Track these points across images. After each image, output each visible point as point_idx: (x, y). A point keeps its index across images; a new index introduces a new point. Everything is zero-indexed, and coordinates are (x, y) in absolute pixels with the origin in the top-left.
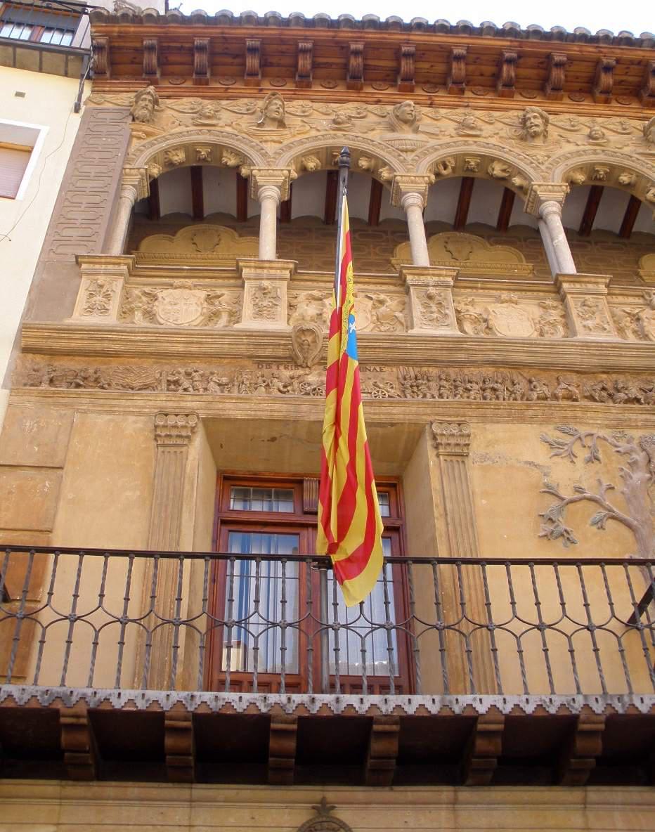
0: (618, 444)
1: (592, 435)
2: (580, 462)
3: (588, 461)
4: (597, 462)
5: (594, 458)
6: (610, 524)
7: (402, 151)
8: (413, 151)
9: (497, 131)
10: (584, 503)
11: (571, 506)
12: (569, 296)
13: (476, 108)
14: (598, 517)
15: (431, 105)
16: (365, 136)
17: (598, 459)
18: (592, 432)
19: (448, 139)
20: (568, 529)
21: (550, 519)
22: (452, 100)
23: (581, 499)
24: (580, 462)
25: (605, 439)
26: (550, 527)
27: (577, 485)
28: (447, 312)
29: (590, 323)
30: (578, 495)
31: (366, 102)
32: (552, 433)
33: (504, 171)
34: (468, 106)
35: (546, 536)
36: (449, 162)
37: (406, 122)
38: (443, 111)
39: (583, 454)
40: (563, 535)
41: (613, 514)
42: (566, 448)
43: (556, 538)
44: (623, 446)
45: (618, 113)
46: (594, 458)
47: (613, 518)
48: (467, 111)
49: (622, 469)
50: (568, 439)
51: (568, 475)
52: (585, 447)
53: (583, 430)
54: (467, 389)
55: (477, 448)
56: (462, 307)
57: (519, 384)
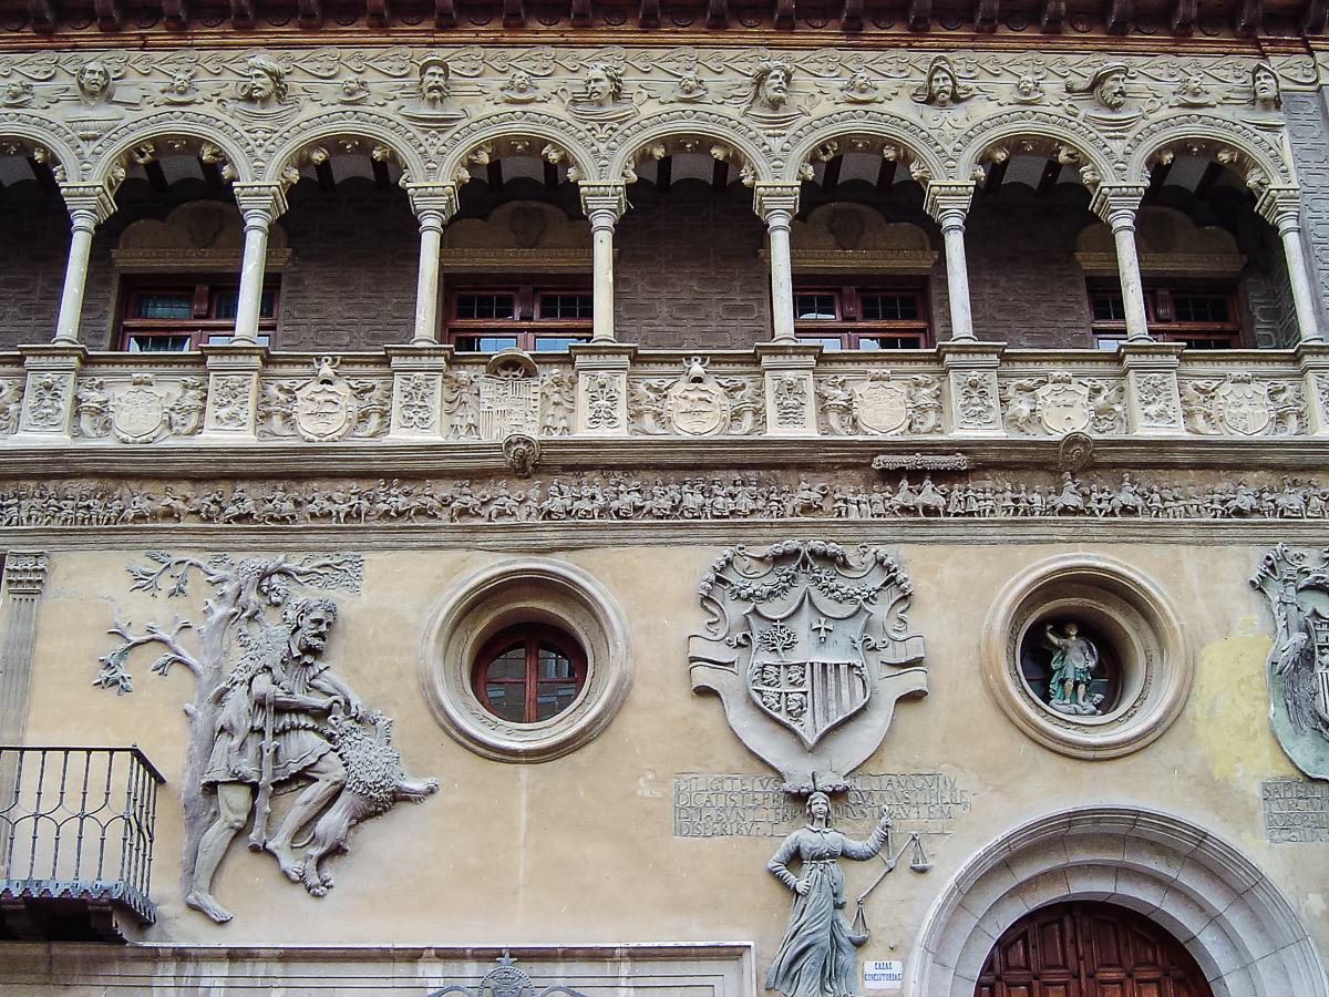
0: (213, 571)
1: (184, 562)
2: (162, 595)
3: (171, 595)
4: (181, 594)
5: (178, 592)
6: (176, 668)
7: (85, 139)
8: (95, 138)
9: (217, 91)
10: (152, 644)
11: (137, 649)
12: (212, 374)
13: (202, 48)
14: (161, 660)
15: (142, 47)
16: (43, 113)
17: (181, 591)
18: (184, 559)
19: (149, 110)
20: (125, 676)
21: (109, 664)
22: (169, 39)
23: (148, 641)
24: (162, 595)
25: (198, 566)
26: (106, 674)
27: (151, 624)
28: (61, 405)
29: (223, 412)
30: (150, 636)
31: (58, 49)
32: (141, 562)
33: (215, 155)
34: (191, 46)
35: (100, 683)
36: (146, 148)
37: (93, 94)
38: (158, 55)
39: (168, 584)
40: (118, 683)
41: (179, 657)
42: (150, 579)
43: (112, 685)
44: (220, 573)
45: (400, 39)
46: (178, 592)
47: (179, 661)
48: (193, 53)
49: (207, 603)
50: (156, 568)
51: (151, 612)
52: (172, 576)
53: (177, 556)
54: (59, 508)
55: (54, 583)
56: (84, 393)
57: (120, 499)
